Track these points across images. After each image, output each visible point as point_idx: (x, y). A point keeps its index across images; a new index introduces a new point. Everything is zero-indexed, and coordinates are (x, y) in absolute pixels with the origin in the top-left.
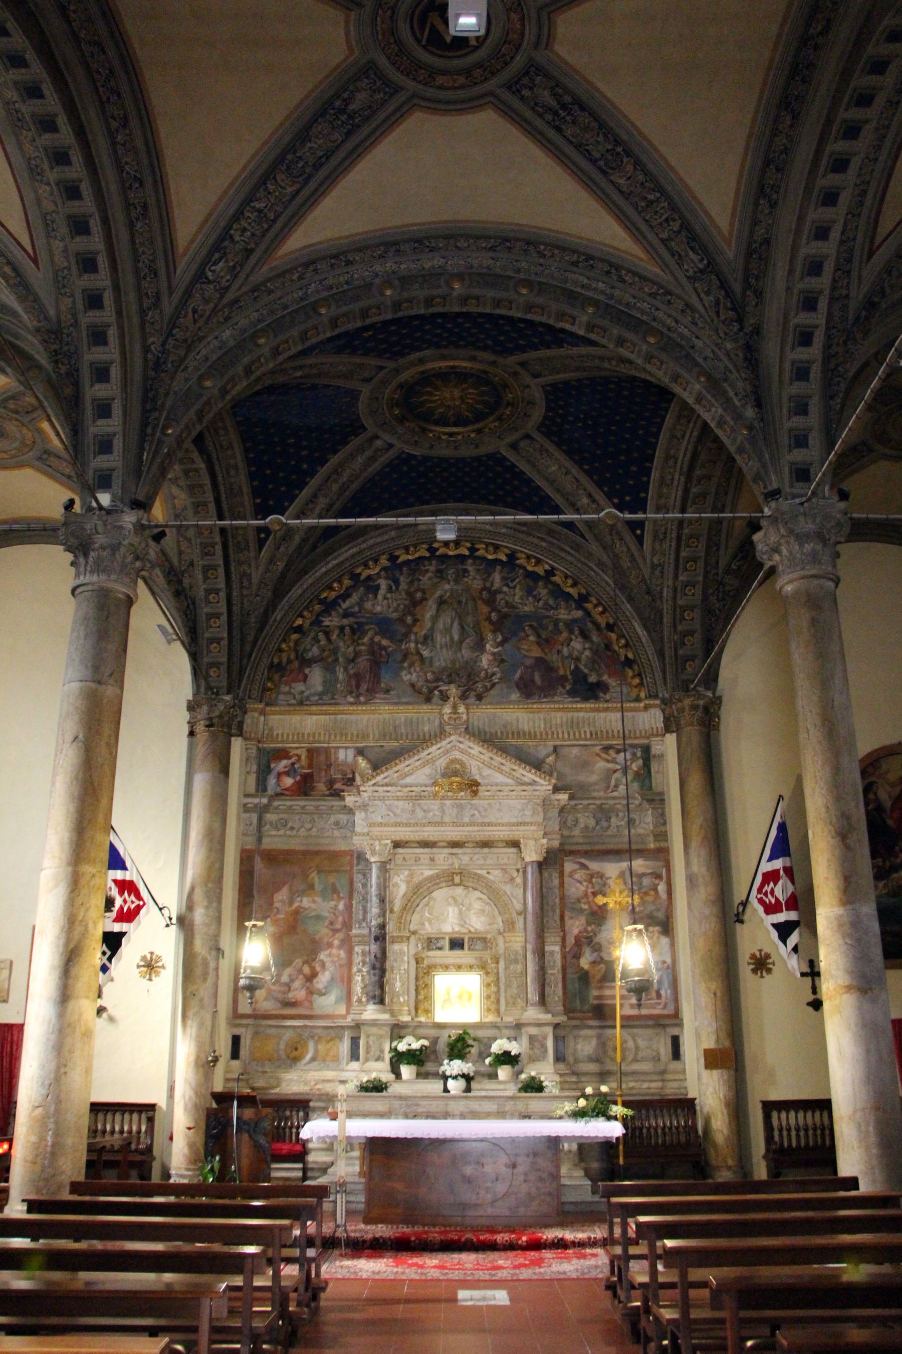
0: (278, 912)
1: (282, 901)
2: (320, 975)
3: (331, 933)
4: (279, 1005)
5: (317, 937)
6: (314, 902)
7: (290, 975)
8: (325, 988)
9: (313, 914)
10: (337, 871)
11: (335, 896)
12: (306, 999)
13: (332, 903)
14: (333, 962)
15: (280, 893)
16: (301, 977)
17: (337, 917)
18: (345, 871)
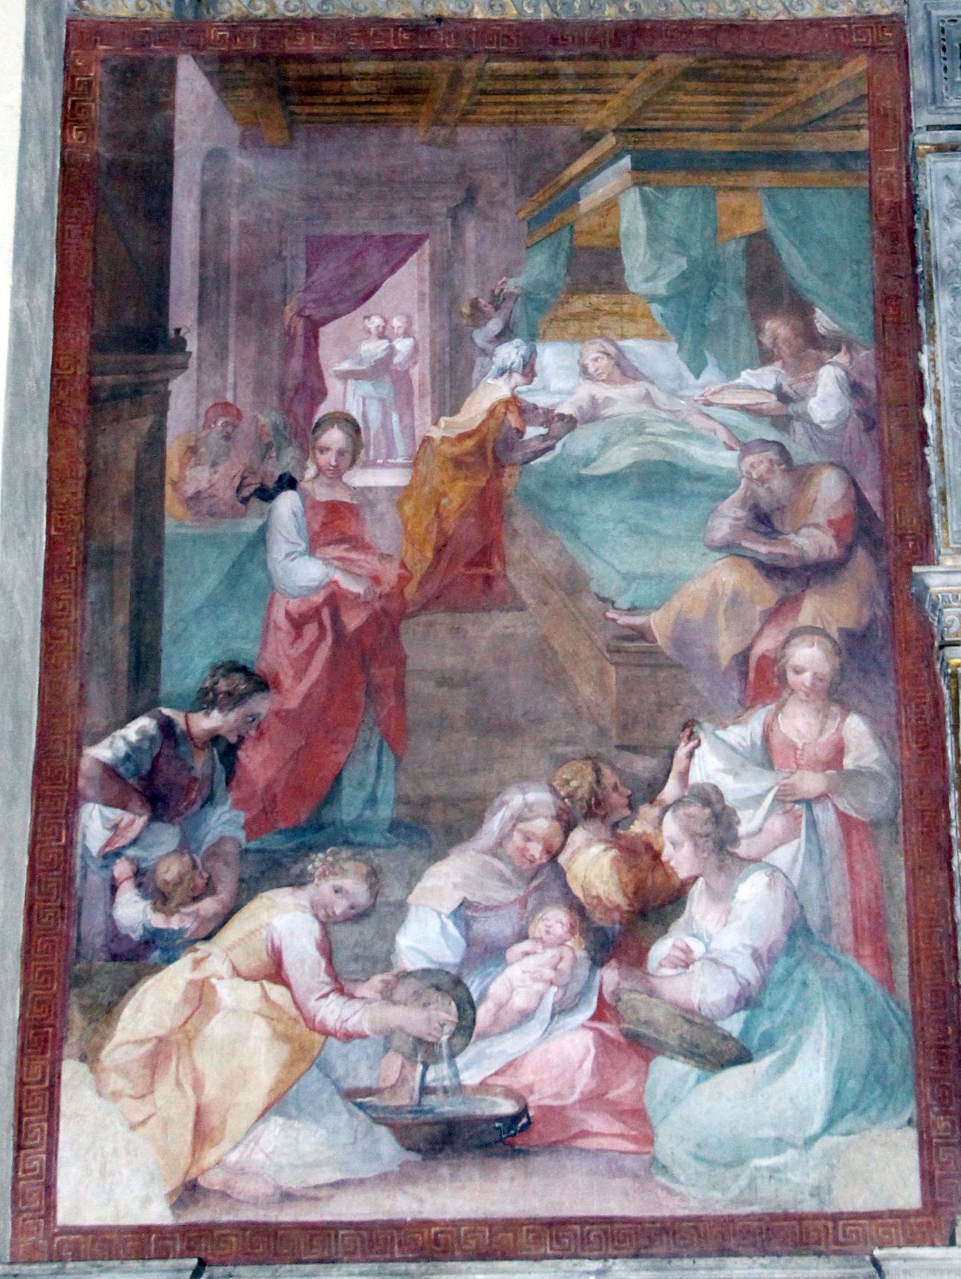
0: (354, 452)
1: (382, 367)
2: (698, 904)
3: (766, 593)
4: (388, 1147)
5: (659, 623)
6: (624, 370)
7: (464, 914)
8: (746, 1001)
9: (621, 457)
10: (780, 160)
11: (777, 328)
12: (594, 1099)
13: (766, 378)
14: (785, 799)
15: (370, 318)
16: (556, 920)
17: (800, 475)
18: (841, 160)
